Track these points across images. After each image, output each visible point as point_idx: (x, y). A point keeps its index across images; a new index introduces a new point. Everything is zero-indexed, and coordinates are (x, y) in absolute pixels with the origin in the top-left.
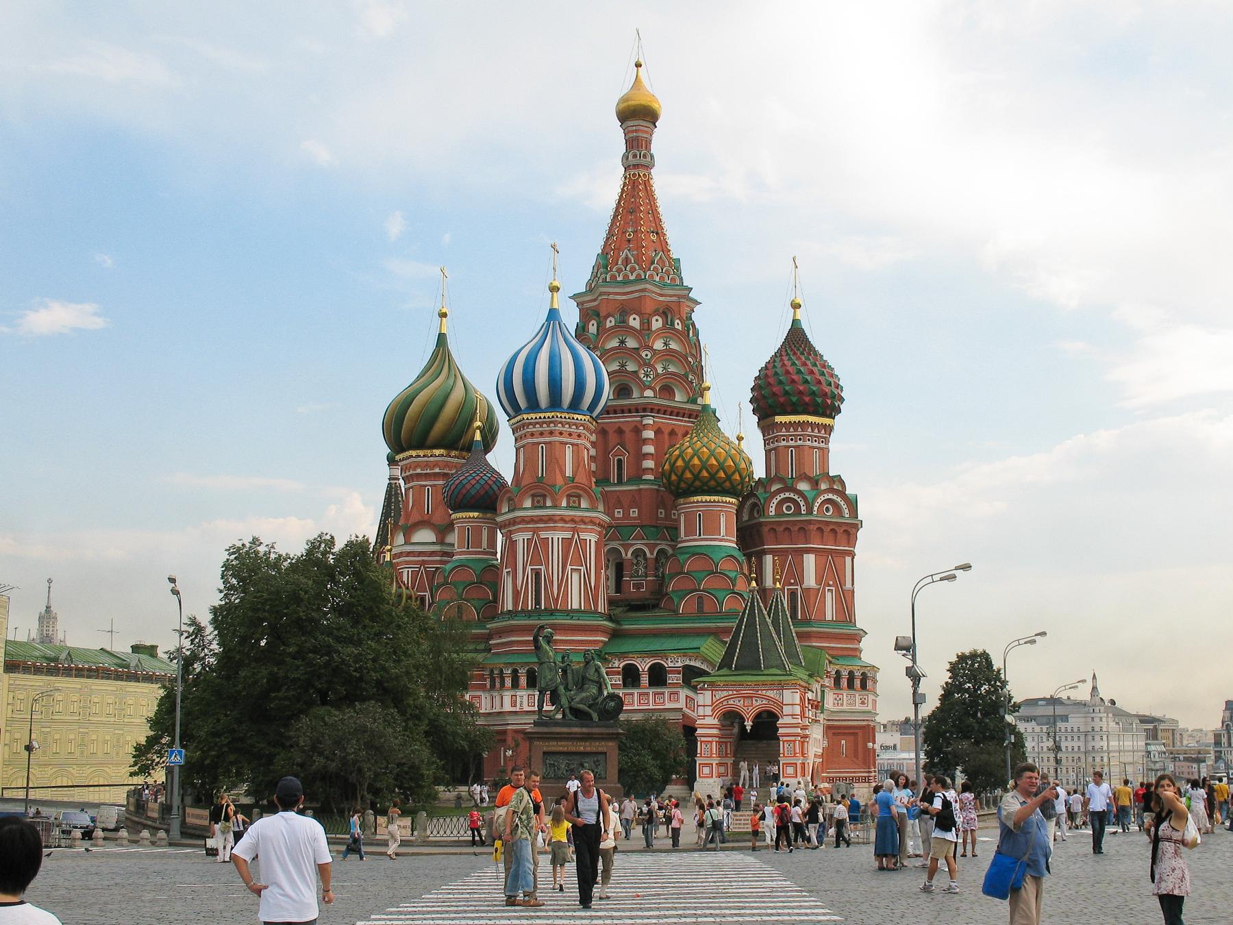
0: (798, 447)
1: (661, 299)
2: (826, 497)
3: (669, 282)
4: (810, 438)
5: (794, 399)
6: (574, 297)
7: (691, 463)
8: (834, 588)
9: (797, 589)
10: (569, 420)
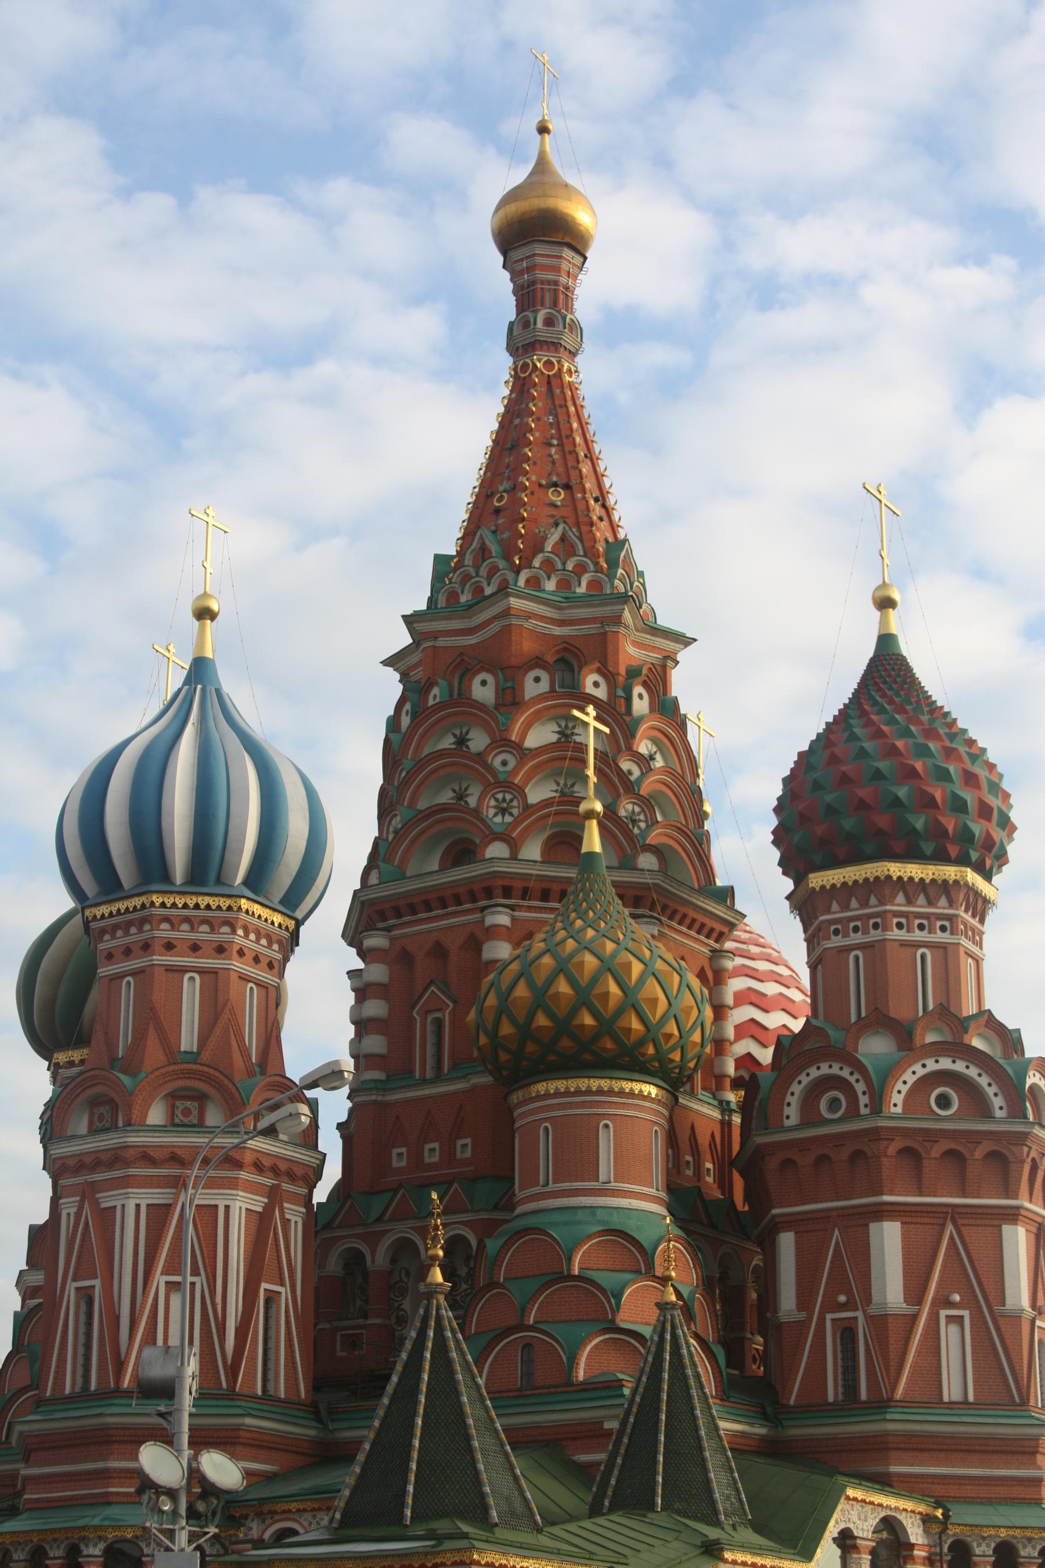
1: (557, 631)
2: (932, 1066)
3: (582, 589)
4: (903, 921)
5: (848, 824)
6: (388, 662)
7: (511, 998)
8: (966, 1313)
9: (856, 1318)
10: (185, 912)
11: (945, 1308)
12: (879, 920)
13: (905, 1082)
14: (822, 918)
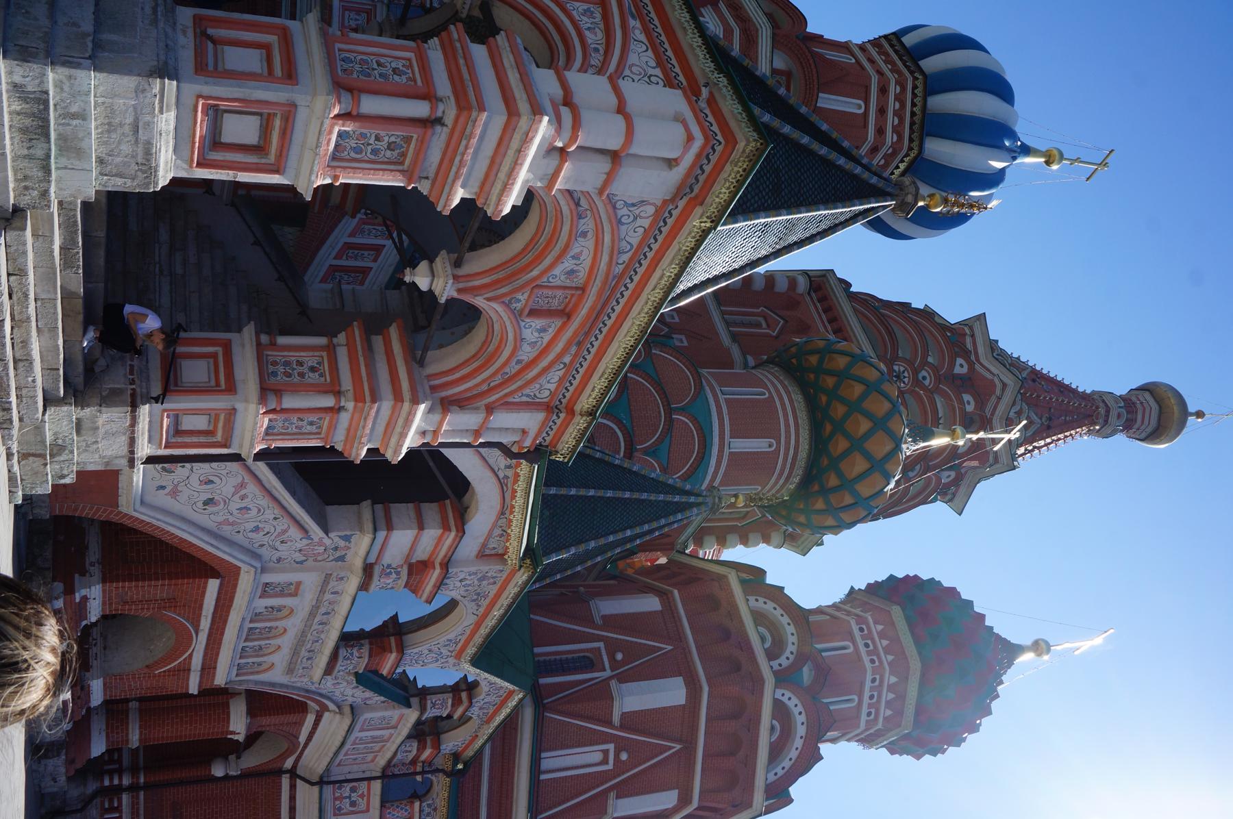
0: (860, 658)
4: (877, 683)
8: (610, 766)
9: (604, 670)
11: (615, 748)
12: (877, 663)
13: (790, 699)
14: (869, 617)
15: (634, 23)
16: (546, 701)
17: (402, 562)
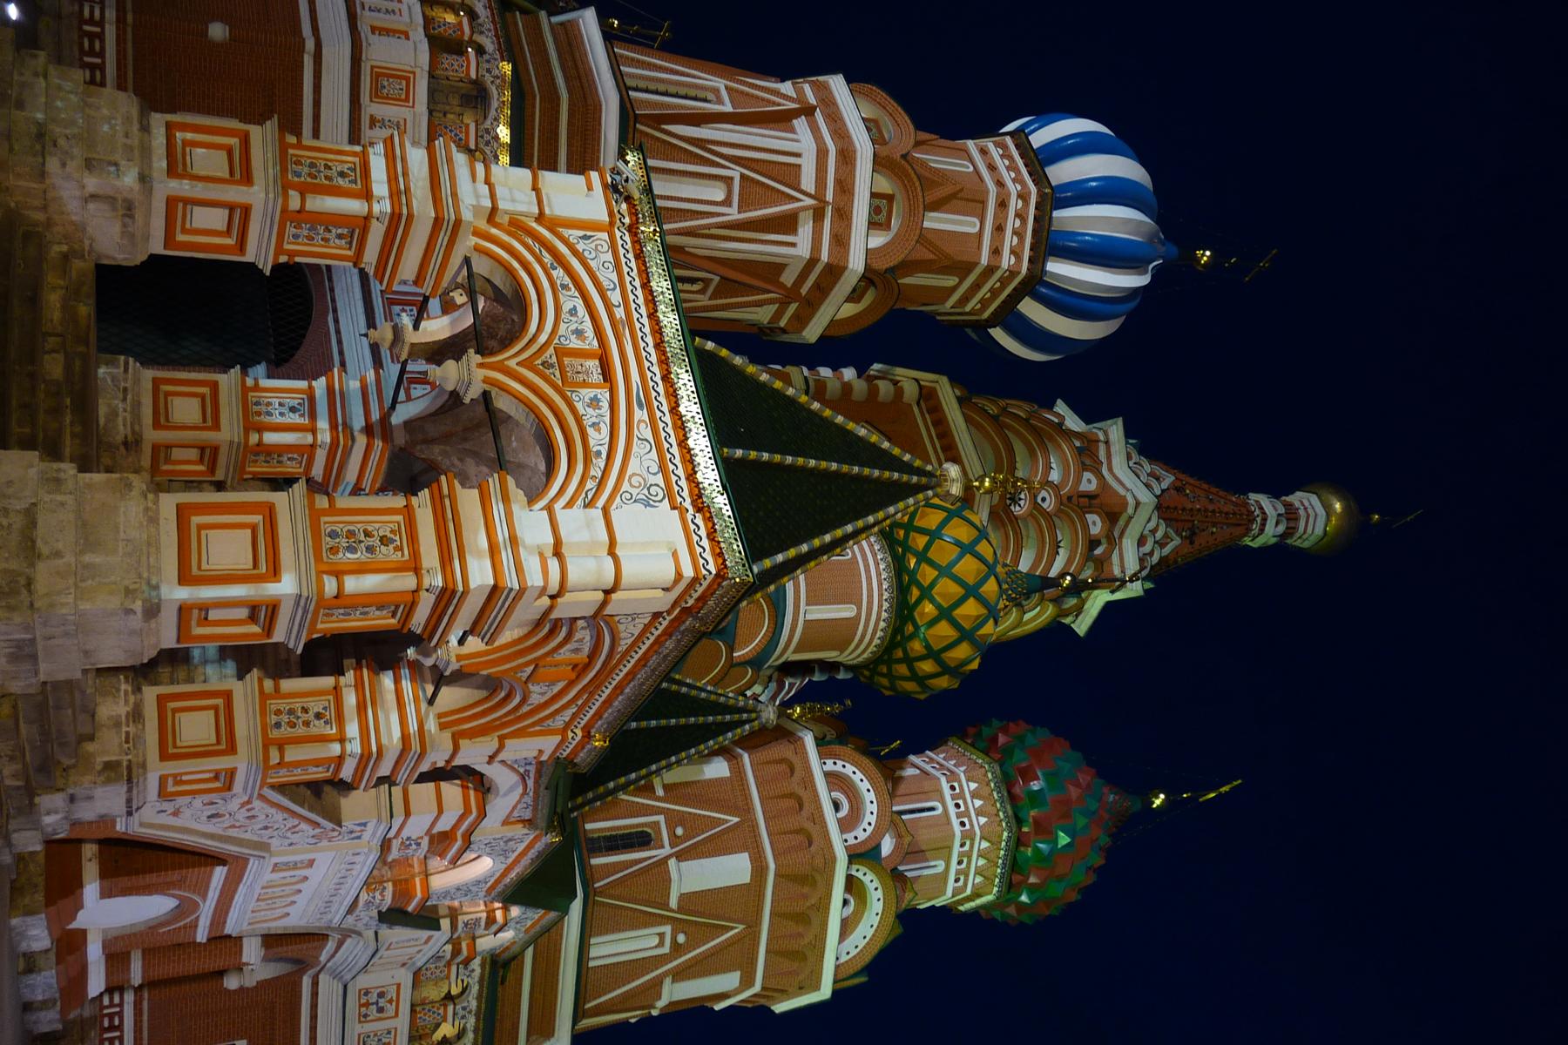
8: (666, 949)
9: (663, 847)
11: (673, 930)
15: (640, 415)
16: (596, 885)
17: (423, 834)
